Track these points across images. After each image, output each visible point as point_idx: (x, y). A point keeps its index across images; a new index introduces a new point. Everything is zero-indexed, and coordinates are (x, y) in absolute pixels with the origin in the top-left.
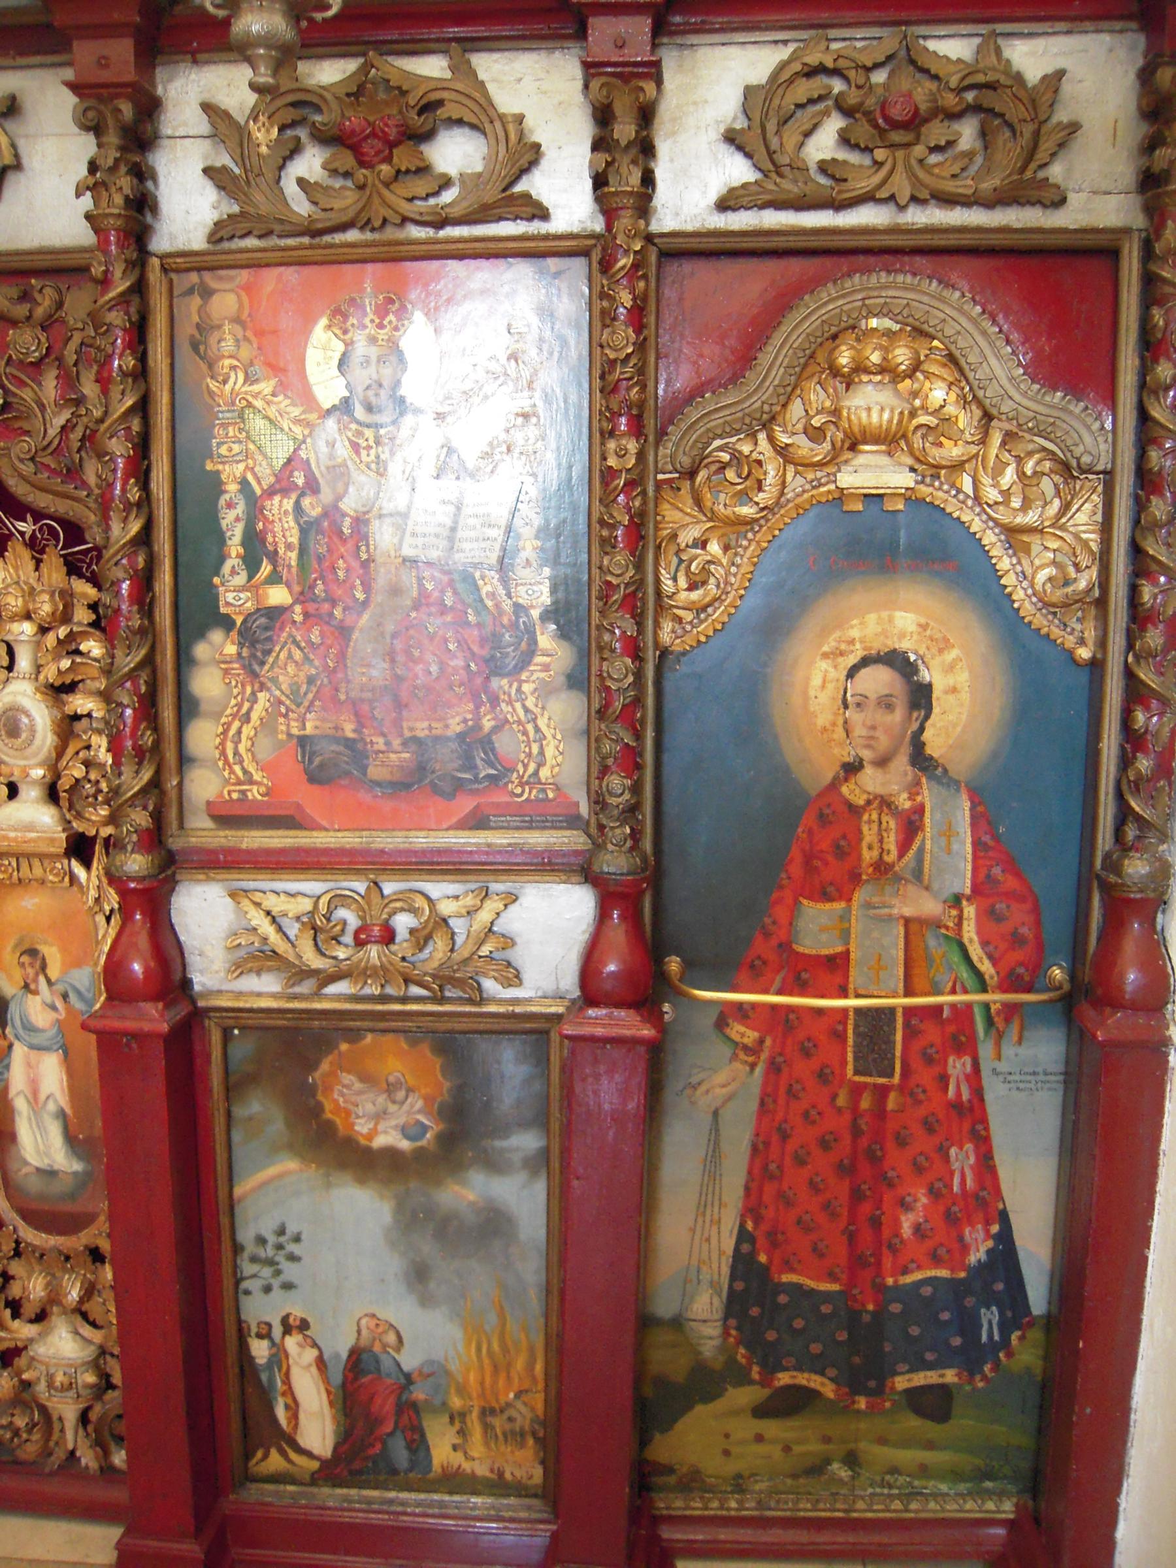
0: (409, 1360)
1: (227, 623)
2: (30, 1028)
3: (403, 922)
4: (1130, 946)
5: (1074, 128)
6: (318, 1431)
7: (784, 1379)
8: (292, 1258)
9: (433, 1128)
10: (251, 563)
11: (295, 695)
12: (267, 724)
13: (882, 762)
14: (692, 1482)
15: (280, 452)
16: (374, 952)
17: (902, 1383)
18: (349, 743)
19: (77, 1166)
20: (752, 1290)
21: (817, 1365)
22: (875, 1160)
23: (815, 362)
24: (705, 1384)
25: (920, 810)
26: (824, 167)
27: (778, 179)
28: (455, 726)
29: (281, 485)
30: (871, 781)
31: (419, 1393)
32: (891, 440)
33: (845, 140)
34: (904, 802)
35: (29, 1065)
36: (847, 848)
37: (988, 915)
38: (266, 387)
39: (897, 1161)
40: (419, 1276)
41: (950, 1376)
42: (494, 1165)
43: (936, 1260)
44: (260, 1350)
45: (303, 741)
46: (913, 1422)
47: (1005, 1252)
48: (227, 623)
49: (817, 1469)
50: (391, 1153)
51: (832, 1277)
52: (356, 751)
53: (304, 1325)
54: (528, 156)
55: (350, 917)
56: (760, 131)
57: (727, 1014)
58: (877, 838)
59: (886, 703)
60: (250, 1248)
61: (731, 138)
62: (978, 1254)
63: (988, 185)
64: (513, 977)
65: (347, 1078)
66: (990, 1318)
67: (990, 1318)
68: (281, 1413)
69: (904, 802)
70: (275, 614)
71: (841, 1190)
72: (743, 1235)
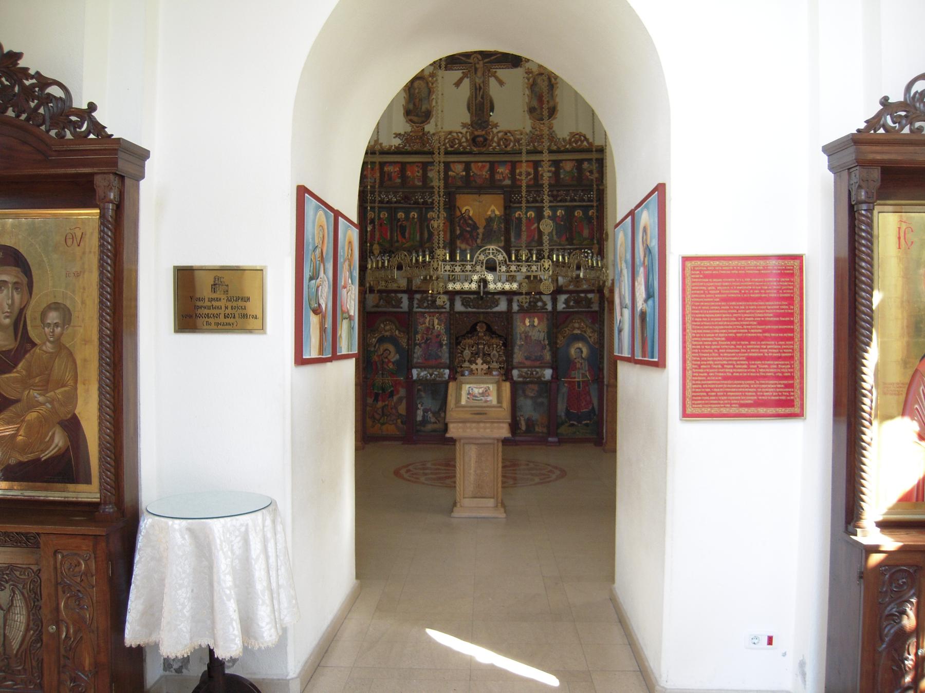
6: (524, 428)
20: (568, 413)
24: (563, 424)
27: (568, 306)
32: (578, 328)
47: (593, 408)
56: (567, 302)
57: (566, 382)
58: (578, 365)
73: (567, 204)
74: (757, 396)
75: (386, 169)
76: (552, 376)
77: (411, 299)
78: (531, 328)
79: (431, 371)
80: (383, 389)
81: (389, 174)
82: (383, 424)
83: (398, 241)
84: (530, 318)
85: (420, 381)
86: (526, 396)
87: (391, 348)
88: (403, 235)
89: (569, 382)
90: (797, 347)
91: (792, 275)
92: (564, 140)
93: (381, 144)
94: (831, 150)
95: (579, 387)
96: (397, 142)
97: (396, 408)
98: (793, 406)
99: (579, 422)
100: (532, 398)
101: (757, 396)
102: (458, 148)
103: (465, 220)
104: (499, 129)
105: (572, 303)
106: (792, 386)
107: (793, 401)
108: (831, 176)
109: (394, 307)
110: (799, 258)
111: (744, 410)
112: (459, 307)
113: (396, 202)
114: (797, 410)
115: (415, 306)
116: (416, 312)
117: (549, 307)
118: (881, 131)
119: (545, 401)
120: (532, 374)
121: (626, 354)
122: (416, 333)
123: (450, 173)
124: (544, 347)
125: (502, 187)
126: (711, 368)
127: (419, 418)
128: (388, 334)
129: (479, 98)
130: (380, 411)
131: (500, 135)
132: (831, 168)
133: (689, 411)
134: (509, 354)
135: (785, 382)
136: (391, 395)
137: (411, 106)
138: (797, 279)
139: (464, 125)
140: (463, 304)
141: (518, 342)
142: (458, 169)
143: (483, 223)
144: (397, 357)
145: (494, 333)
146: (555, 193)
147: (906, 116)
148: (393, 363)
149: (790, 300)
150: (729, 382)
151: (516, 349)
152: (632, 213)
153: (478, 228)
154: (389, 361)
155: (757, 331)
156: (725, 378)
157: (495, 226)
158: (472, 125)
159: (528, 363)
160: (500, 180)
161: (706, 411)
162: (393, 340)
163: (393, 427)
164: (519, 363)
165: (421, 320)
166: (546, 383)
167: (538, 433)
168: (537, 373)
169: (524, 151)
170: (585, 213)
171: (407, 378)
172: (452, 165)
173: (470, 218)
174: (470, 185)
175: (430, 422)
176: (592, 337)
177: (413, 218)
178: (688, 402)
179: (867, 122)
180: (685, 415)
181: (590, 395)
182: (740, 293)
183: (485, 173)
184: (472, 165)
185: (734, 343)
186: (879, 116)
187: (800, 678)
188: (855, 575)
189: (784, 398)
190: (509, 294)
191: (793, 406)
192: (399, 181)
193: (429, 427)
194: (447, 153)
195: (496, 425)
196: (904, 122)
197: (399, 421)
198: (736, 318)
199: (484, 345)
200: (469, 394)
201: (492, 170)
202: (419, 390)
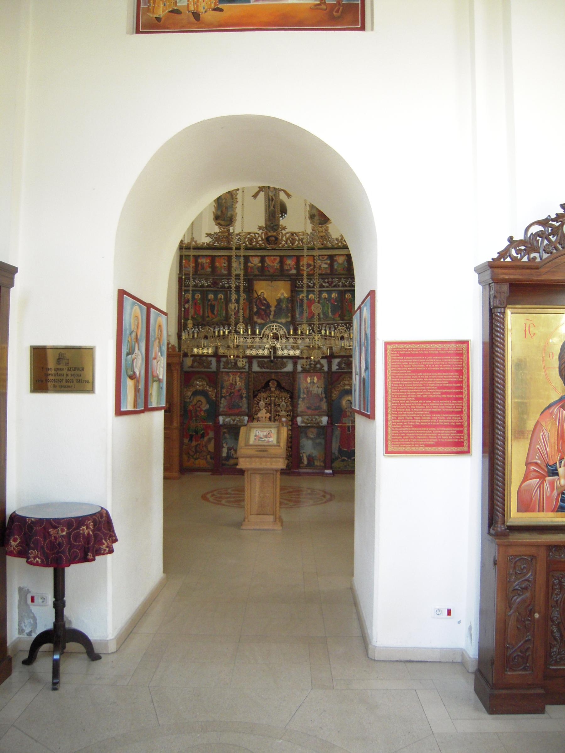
6: (305, 462)
20: (340, 450)
21: (346, 457)
24: (337, 458)
27: (340, 368)
44: (301, 455)
49: (345, 466)
54: (323, 366)
56: (339, 364)
57: (339, 426)
73: (340, 289)
74: (438, 439)
75: (199, 260)
76: (328, 423)
79: (233, 418)
80: (196, 432)
81: (202, 265)
82: (196, 459)
83: (208, 317)
84: (311, 377)
85: (225, 425)
86: (308, 438)
88: (213, 312)
89: (341, 427)
90: (465, 404)
91: (461, 354)
92: (337, 239)
93: (196, 242)
94: (479, 270)
95: (349, 430)
96: (207, 240)
97: (206, 446)
98: (463, 446)
100: (312, 439)
101: (438, 439)
102: (255, 245)
103: (261, 301)
104: (287, 231)
105: (343, 366)
106: (462, 432)
107: (463, 442)
108: (479, 288)
109: (205, 367)
110: (467, 342)
111: (428, 449)
113: (207, 287)
114: (465, 449)
115: (222, 366)
116: (223, 372)
117: (326, 369)
118: (508, 259)
119: (323, 441)
120: (312, 420)
121: (357, 409)
122: (222, 388)
123: (250, 264)
124: (321, 400)
125: (289, 276)
126: (405, 419)
127: (224, 454)
128: (201, 388)
129: (272, 208)
130: (193, 449)
131: (288, 235)
132: (480, 282)
133: (390, 449)
134: (294, 405)
135: (457, 429)
136: (203, 436)
137: (219, 213)
138: (465, 357)
139: (260, 228)
140: (259, 366)
141: (302, 396)
142: (256, 261)
143: (275, 303)
144: (208, 406)
145: (283, 388)
147: (524, 250)
148: (205, 411)
149: (460, 372)
150: (418, 429)
151: (300, 402)
152: (359, 308)
154: (201, 410)
155: (437, 393)
156: (415, 426)
157: (284, 306)
158: (266, 228)
159: (310, 412)
160: (287, 270)
161: (402, 449)
162: (204, 393)
164: (303, 412)
165: (226, 378)
166: (323, 428)
168: (316, 419)
169: (305, 248)
172: (251, 259)
173: (265, 299)
174: (264, 273)
177: (221, 299)
178: (389, 443)
179: (498, 253)
180: (387, 452)
182: (425, 367)
183: (276, 265)
184: (267, 258)
185: (421, 402)
186: (507, 250)
187: (469, 639)
188: (492, 563)
189: (456, 440)
190: (295, 359)
191: (463, 446)
192: (209, 270)
194: (247, 249)
195: (274, 459)
196: (523, 254)
197: (209, 457)
198: (422, 384)
199: (275, 397)
200: (256, 436)
201: (282, 262)
202: (224, 433)
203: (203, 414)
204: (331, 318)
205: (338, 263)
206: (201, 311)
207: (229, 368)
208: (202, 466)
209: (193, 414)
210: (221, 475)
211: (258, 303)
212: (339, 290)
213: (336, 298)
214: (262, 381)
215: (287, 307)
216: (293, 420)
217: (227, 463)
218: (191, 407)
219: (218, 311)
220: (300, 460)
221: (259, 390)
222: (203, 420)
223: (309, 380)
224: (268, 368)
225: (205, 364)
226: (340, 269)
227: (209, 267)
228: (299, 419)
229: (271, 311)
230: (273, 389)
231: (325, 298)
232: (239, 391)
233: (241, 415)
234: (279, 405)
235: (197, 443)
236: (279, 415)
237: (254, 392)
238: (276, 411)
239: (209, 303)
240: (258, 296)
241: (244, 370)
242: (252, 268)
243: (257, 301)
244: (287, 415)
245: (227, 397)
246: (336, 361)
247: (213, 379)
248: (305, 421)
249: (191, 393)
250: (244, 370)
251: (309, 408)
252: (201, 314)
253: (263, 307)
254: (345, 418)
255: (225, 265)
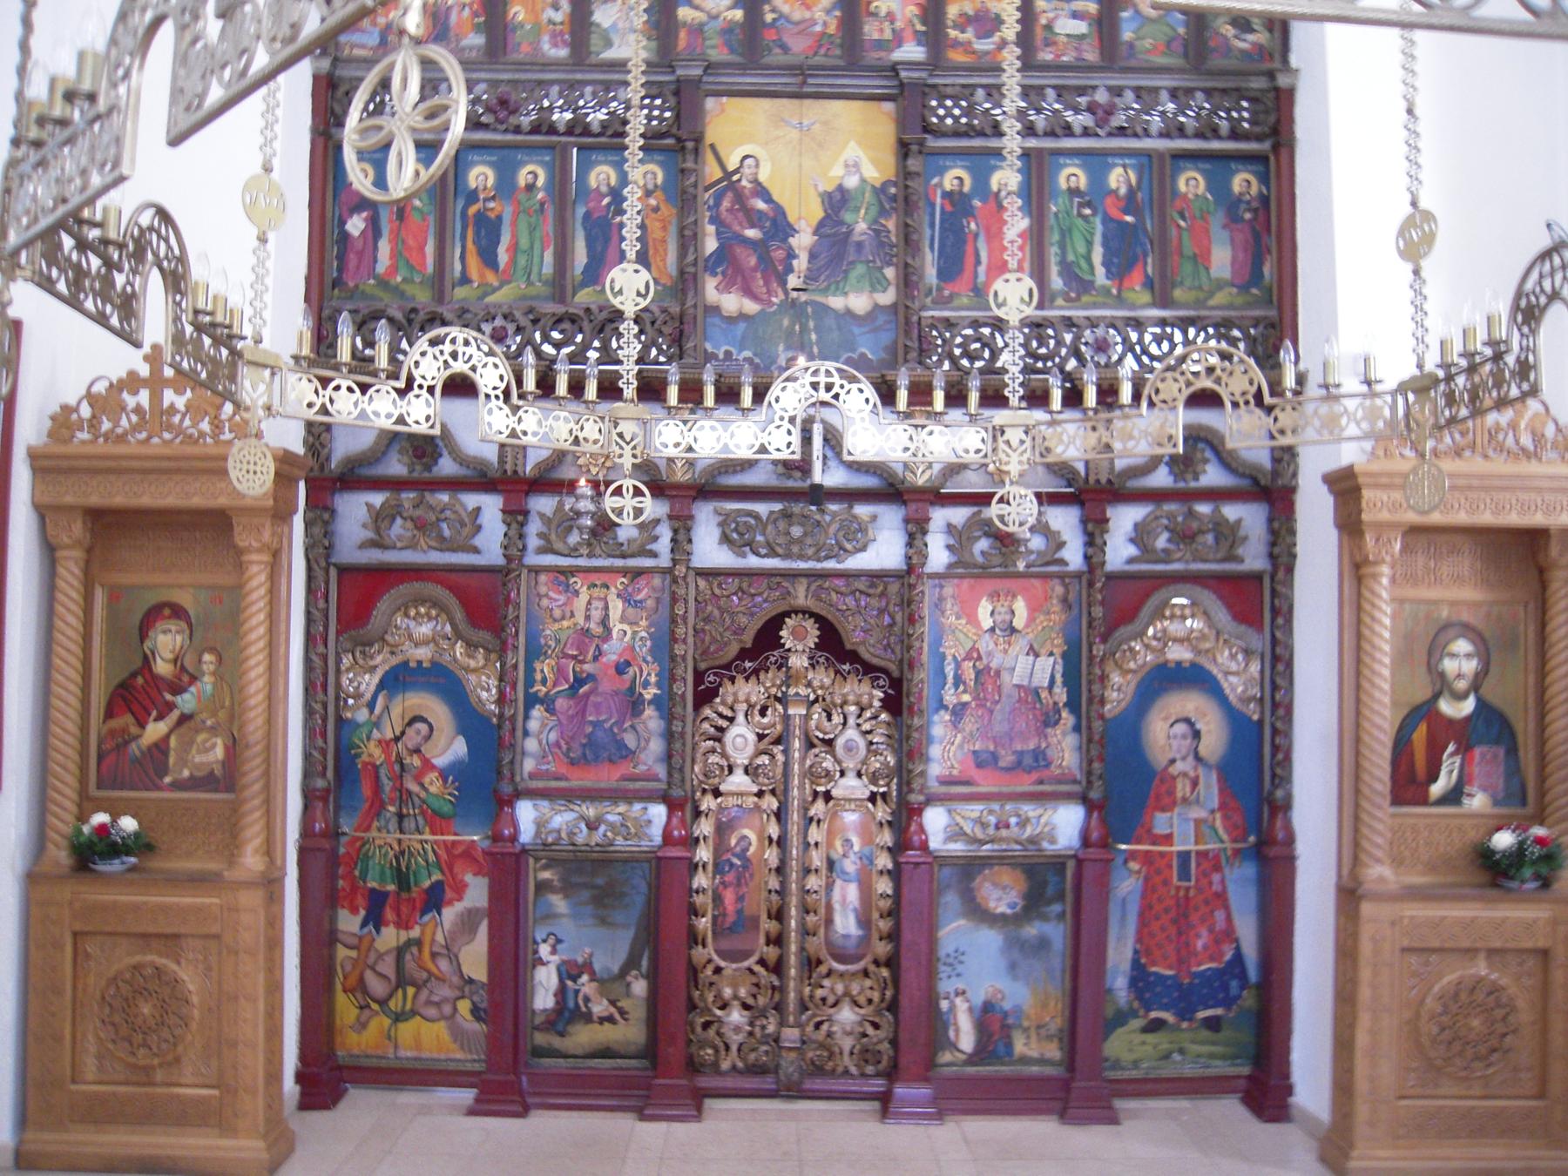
0: (1007, 1005)
1: (946, 708)
2: (844, 872)
3: (1013, 820)
4: (1279, 823)
5: (1245, 538)
6: (966, 1039)
7: (1153, 1015)
8: (961, 962)
9: (1021, 903)
10: (956, 686)
11: (971, 734)
12: (961, 746)
13: (1184, 758)
14: (1116, 1065)
15: (968, 646)
16: (1004, 833)
17: (1202, 1014)
18: (992, 753)
19: (860, 933)
20: (1140, 978)
21: (1165, 1008)
22: (1186, 917)
23: (1159, 614)
24: (1121, 1018)
25: (1197, 777)
26: (1164, 550)
28: (1032, 747)
29: (968, 657)
30: (1180, 766)
31: (1010, 1021)
33: (1169, 540)
34: (1192, 774)
35: (842, 888)
36: (1171, 792)
37: (1225, 818)
38: (963, 621)
39: (1194, 918)
40: (1012, 967)
41: (1219, 1011)
42: (1044, 918)
43: (1212, 959)
44: (944, 1005)
45: (974, 752)
46: (1205, 1034)
47: (1238, 957)
48: (946, 708)
49: (1167, 1056)
50: (1003, 915)
51: (1170, 968)
52: (995, 757)
53: (964, 992)
54: (1061, 545)
55: (992, 820)
56: (1140, 535)
57: (1132, 855)
58: (1182, 788)
59: (1184, 737)
60: (943, 959)
61: (1132, 540)
62: (1228, 956)
63: (1219, 556)
64: (1053, 841)
65: (987, 884)
66: (1234, 984)
67: (1234, 984)
68: (952, 1034)
69: (1192, 774)
70: (965, 705)
71: (1173, 931)
72: (1136, 952)
73: (1147, 144)
77: (515, 515)
78: (994, 642)
79: (591, 811)
82: (398, 1018)
83: (465, 280)
84: (995, 596)
86: (979, 913)
87: (437, 710)
88: (488, 258)
89: (1147, 858)
95: (1184, 874)
97: (454, 959)
99: (1185, 1014)
103: (739, 197)
112: (709, 550)
115: (533, 542)
116: (536, 570)
117: (1073, 555)
119: (1056, 932)
120: (1002, 825)
122: (535, 652)
124: (1049, 720)
127: (544, 1000)
128: (423, 654)
134: (909, 752)
136: (434, 900)
140: (725, 539)
141: (950, 697)
143: (817, 213)
144: (460, 748)
145: (853, 657)
146: (1101, 97)
148: (443, 775)
151: (939, 726)
153: (790, 230)
157: (862, 226)
160: (880, 44)
163: (441, 1028)
164: (947, 781)
166: (1057, 863)
167: (1025, 1060)
168: (1023, 823)
170: (1218, 185)
171: (496, 838)
173: (762, 191)
175: (588, 1018)
176: (1239, 675)
177: (530, 188)
181: (1227, 908)
193: (583, 1037)
197: (464, 1006)
203: (433, 783)
204: (1107, 291)
205: (1137, 12)
206: (430, 249)
207: (573, 552)
208: (426, 1055)
209: (387, 785)
210: (523, 1112)
211: (726, 204)
212: (1147, 154)
213: (1132, 192)
214: (744, 620)
215: (878, 232)
216: (904, 818)
217: (557, 1042)
218: (373, 752)
219: (514, 248)
220: (936, 1027)
221: (727, 667)
222: (437, 820)
223: (984, 609)
224: (773, 553)
225: (447, 533)
226: (1147, 43)
227: (477, 28)
228: (935, 821)
229: (791, 255)
230: (798, 662)
231: (1074, 192)
232: (621, 668)
233: (629, 797)
234: (829, 743)
235: (404, 936)
236: (828, 796)
237: (699, 676)
238: (812, 774)
239: (472, 210)
240: (728, 175)
241: (648, 563)
242: (698, 30)
243: (719, 198)
244: (872, 798)
245: (561, 703)
246: (1124, 519)
247: (485, 603)
248: (968, 828)
249: (376, 680)
250: (648, 563)
251: (985, 761)
252: (430, 269)
253: (751, 233)
254: (1163, 810)
255: (558, 17)
